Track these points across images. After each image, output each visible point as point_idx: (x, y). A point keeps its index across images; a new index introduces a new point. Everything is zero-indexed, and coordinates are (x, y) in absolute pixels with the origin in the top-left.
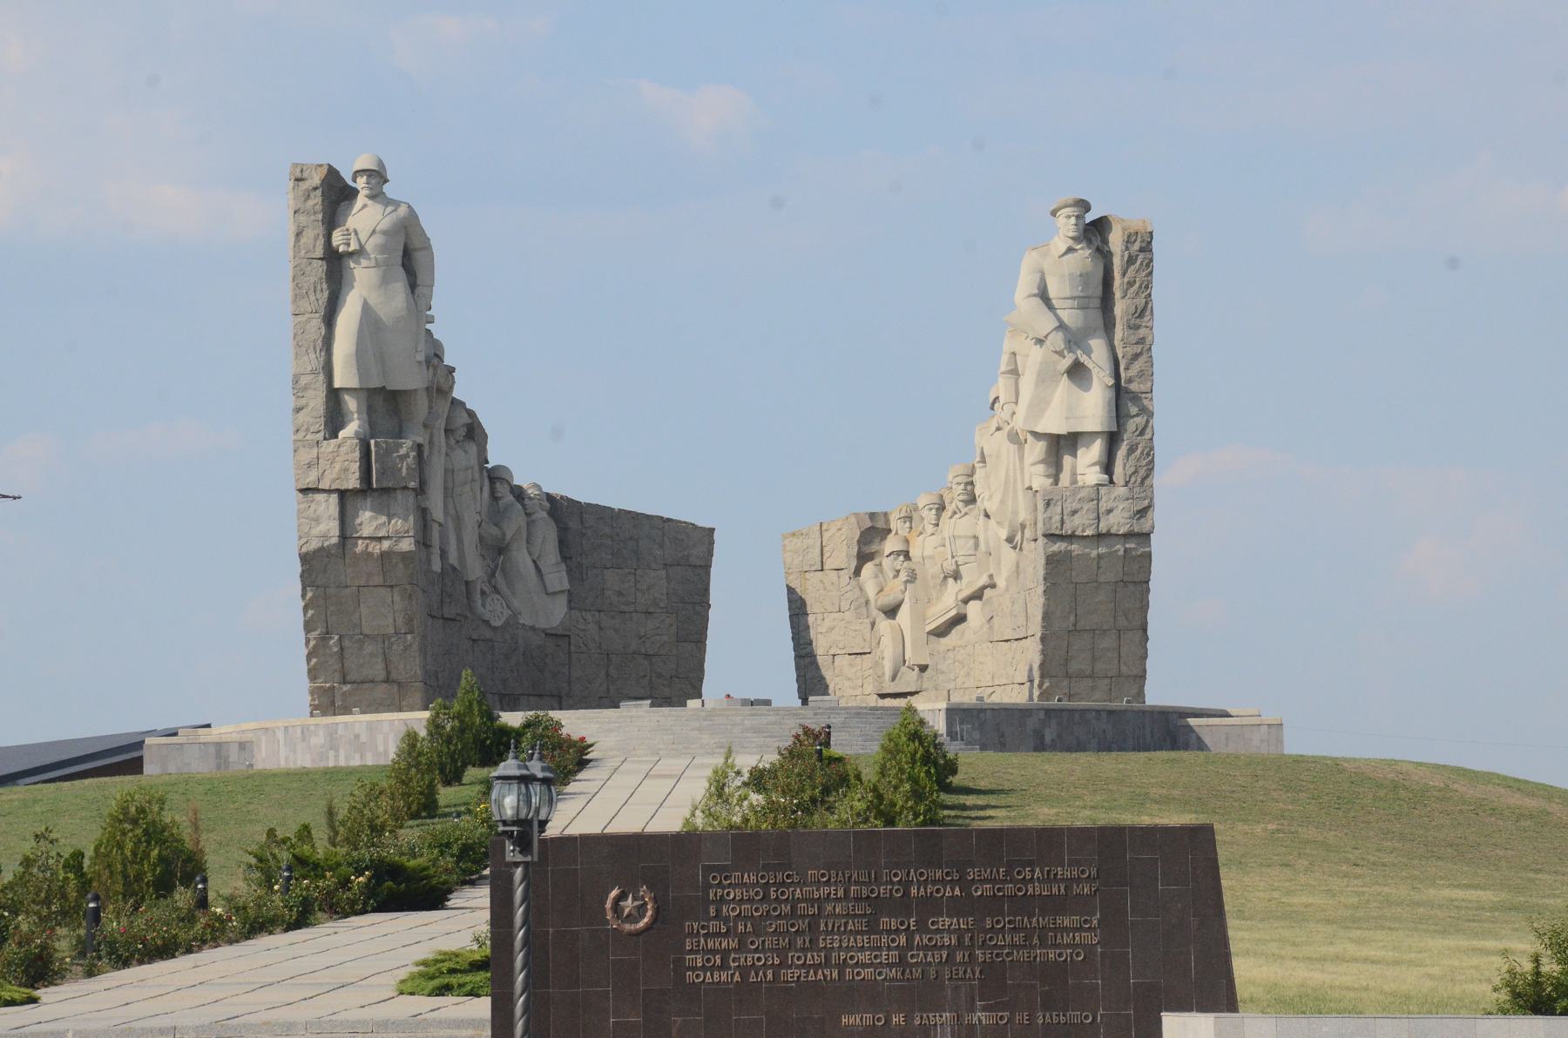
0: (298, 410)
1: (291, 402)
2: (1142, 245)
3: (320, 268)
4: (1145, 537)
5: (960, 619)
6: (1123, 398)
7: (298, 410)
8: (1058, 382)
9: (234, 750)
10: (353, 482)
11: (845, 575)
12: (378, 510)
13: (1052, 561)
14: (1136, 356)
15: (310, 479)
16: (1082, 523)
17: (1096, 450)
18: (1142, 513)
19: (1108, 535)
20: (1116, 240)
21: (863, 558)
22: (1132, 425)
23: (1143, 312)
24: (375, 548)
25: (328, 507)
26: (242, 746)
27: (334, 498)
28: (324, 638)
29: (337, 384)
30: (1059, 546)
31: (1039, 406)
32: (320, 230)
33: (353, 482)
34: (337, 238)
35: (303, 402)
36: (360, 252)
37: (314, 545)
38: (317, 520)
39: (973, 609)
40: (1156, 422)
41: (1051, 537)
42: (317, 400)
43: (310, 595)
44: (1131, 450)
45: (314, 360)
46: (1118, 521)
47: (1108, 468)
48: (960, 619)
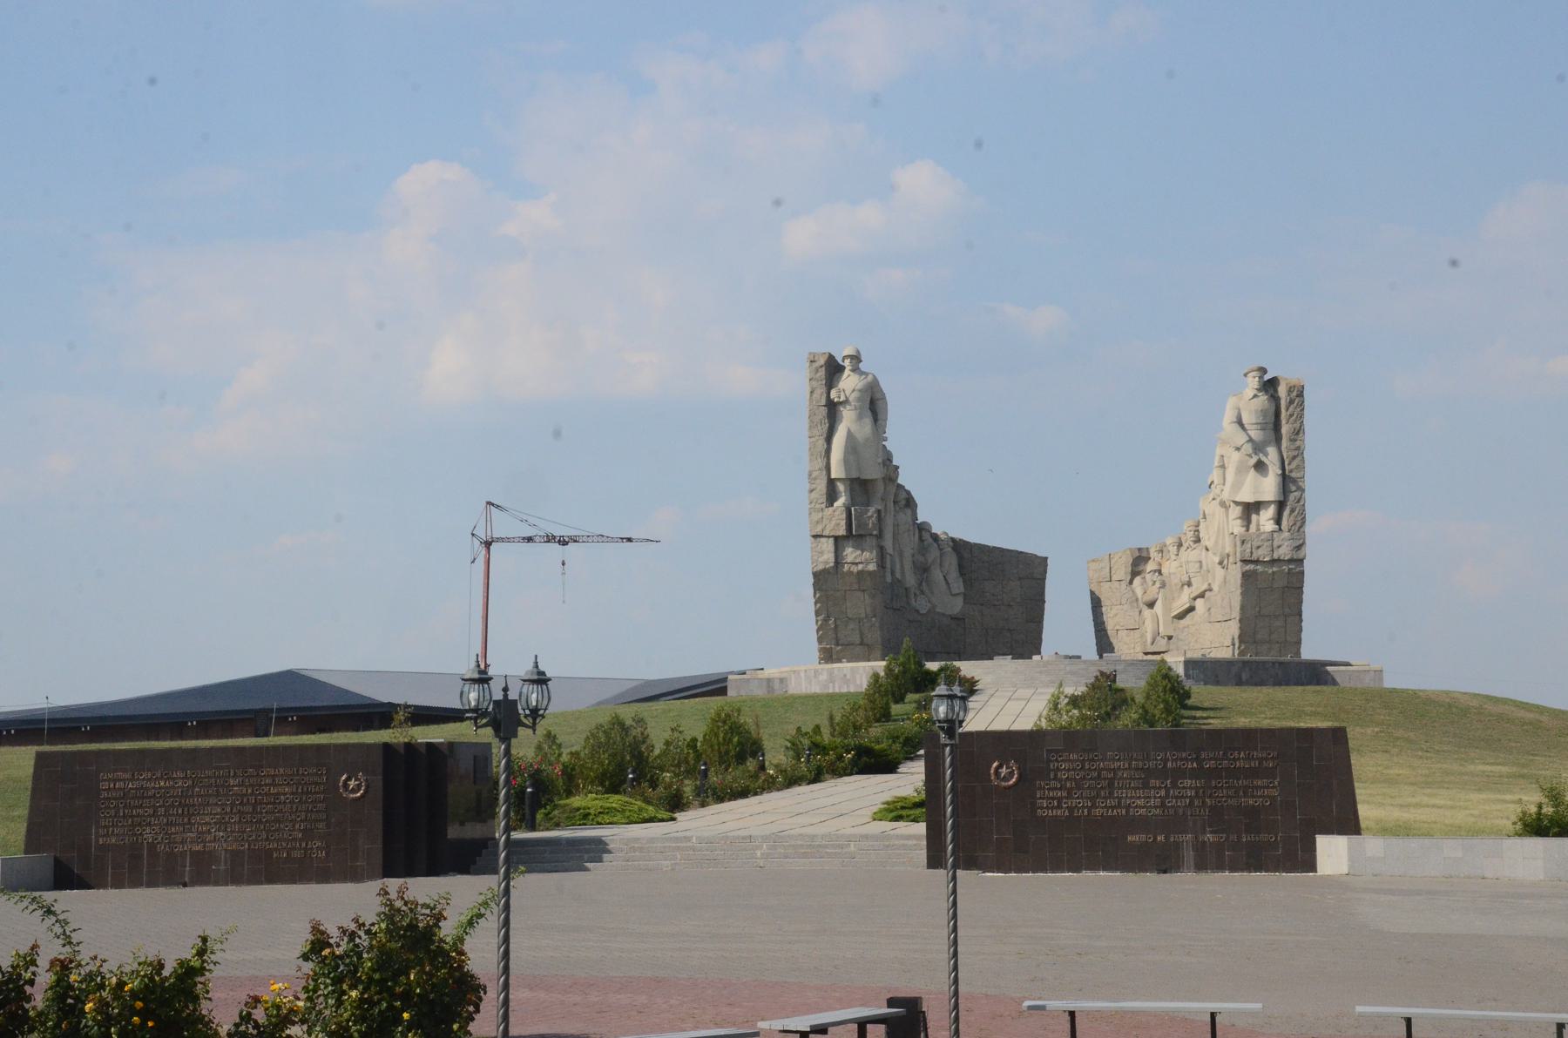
1: (808, 487)
2: (1298, 393)
3: (824, 411)
4: (1301, 561)
5: (1191, 609)
9: (777, 686)
10: (842, 532)
11: (1124, 585)
12: (856, 547)
13: (1246, 576)
14: (1294, 457)
15: (818, 530)
16: (1263, 554)
17: (1270, 511)
18: (1299, 547)
19: (1279, 560)
20: (1282, 391)
21: (1135, 573)
22: (1292, 497)
23: (1298, 432)
24: (855, 569)
25: (828, 546)
26: (782, 680)
27: (831, 541)
28: (826, 620)
29: (833, 476)
30: (1251, 567)
31: (1237, 486)
32: (824, 389)
33: (842, 532)
34: (833, 394)
36: (846, 402)
37: (821, 567)
38: (822, 553)
39: (1199, 603)
40: (1306, 494)
41: (1244, 561)
42: (822, 486)
44: (1292, 511)
45: (820, 463)
46: (1284, 552)
47: (1278, 521)
48: (1191, 609)
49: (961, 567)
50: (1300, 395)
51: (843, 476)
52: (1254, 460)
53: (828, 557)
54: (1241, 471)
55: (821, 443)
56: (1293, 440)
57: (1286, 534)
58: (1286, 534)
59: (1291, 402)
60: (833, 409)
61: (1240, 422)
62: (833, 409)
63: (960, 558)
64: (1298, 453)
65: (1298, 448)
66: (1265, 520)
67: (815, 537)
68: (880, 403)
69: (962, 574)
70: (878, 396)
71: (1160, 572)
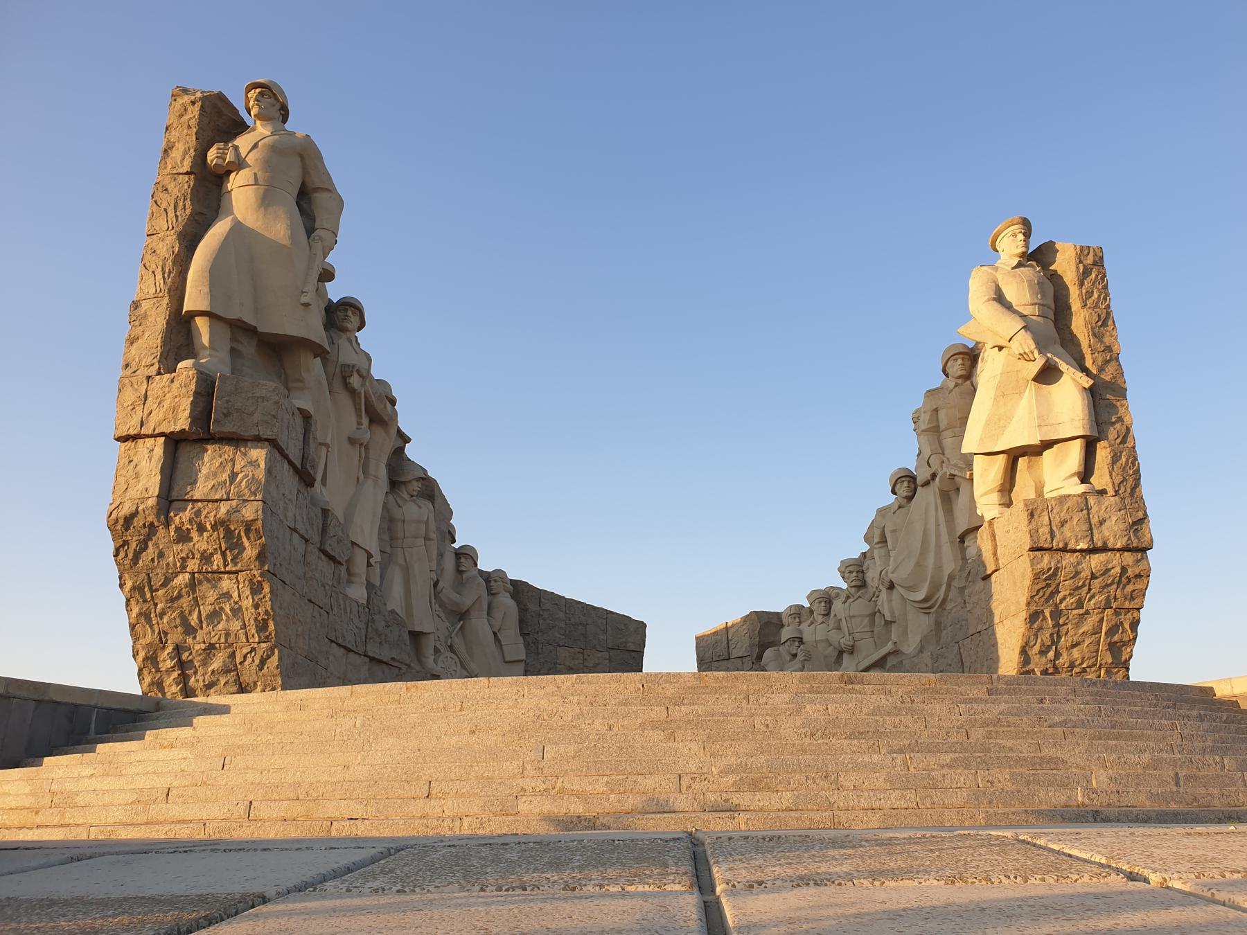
0: (132, 341)
1: (125, 330)
2: (1093, 265)
6: (1104, 400)
7: (132, 341)
8: (1021, 394)
10: (182, 422)
17: (1075, 452)
23: (1104, 321)
25: (151, 456)
30: (1046, 560)
33: (182, 422)
35: (138, 331)
43: (129, 584)
44: (1115, 458)
47: (1085, 475)
49: (522, 622)
50: (1099, 262)
51: (203, 306)
52: (1035, 367)
53: (150, 481)
54: (1006, 393)
55: (167, 245)
56: (1098, 336)
57: (1110, 500)
58: (1110, 500)
59: (1086, 273)
60: (209, 188)
61: (999, 298)
62: (209, 188)
63: (523, 610)
64: (1110, 356)
65: (1108, 349)
66: (1058, 475)
67: (123, 439)
68: (320, 197)
69: (524, 634)
70: (315, 181)
71: (801, 641)
